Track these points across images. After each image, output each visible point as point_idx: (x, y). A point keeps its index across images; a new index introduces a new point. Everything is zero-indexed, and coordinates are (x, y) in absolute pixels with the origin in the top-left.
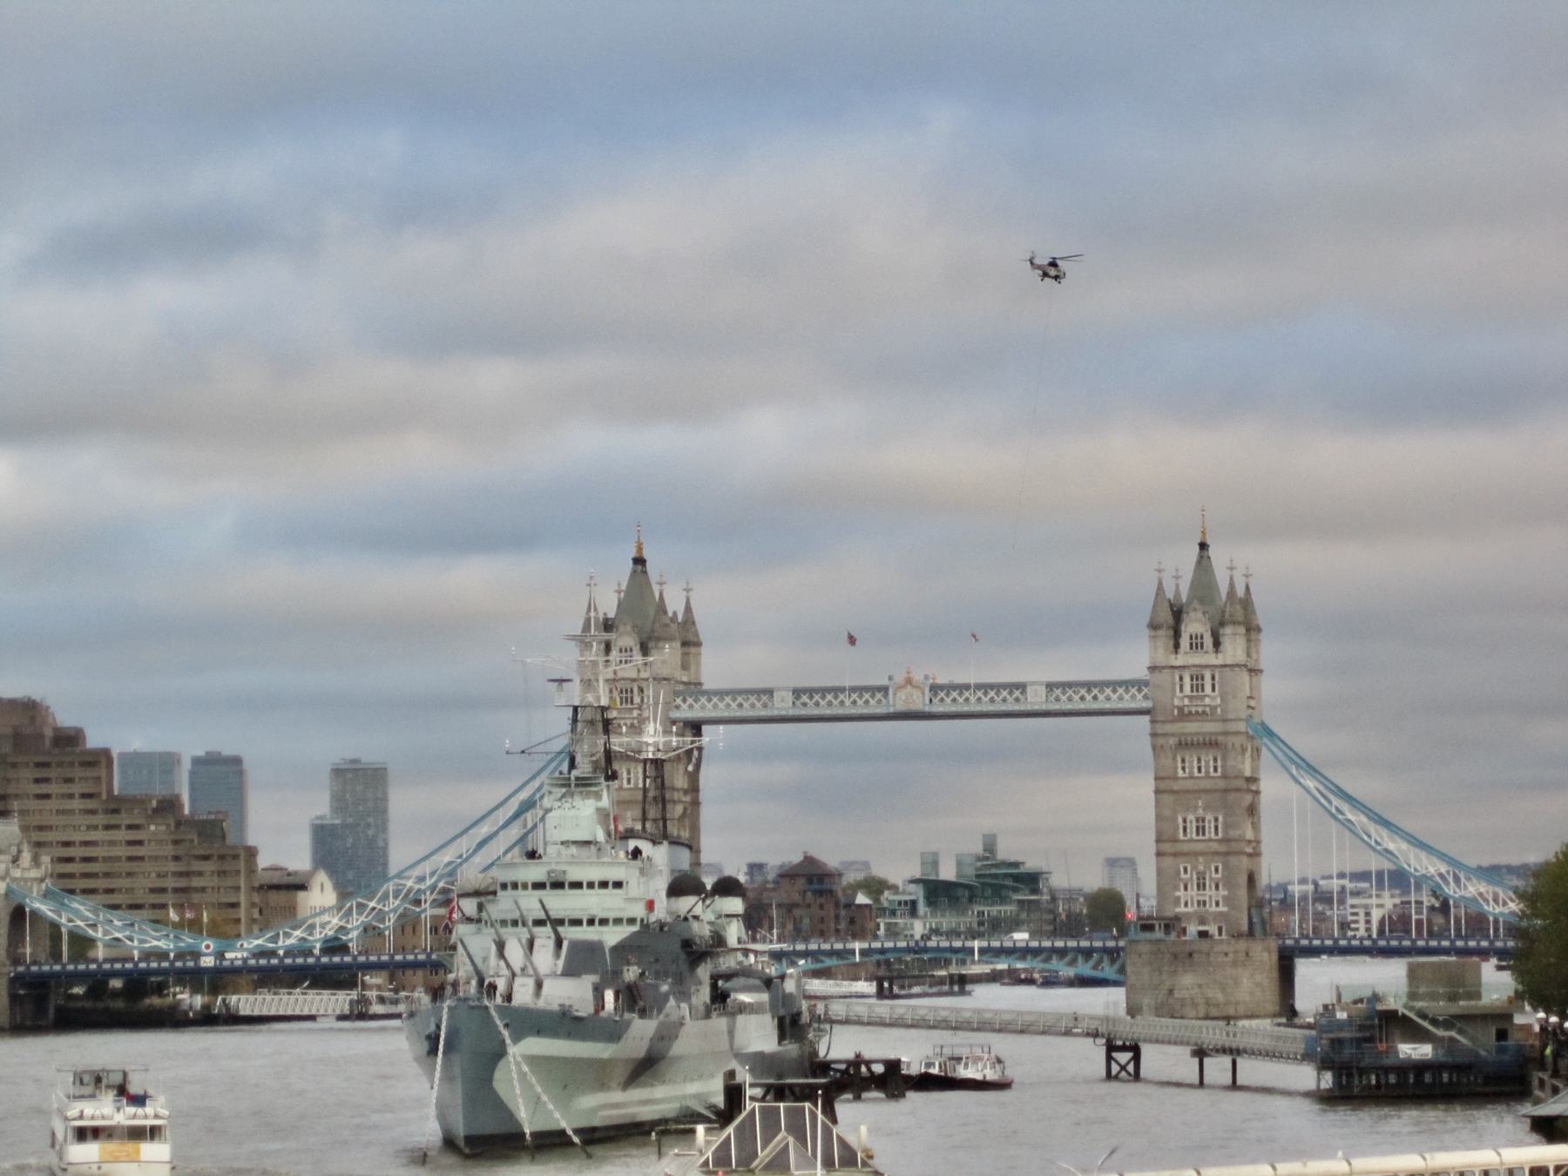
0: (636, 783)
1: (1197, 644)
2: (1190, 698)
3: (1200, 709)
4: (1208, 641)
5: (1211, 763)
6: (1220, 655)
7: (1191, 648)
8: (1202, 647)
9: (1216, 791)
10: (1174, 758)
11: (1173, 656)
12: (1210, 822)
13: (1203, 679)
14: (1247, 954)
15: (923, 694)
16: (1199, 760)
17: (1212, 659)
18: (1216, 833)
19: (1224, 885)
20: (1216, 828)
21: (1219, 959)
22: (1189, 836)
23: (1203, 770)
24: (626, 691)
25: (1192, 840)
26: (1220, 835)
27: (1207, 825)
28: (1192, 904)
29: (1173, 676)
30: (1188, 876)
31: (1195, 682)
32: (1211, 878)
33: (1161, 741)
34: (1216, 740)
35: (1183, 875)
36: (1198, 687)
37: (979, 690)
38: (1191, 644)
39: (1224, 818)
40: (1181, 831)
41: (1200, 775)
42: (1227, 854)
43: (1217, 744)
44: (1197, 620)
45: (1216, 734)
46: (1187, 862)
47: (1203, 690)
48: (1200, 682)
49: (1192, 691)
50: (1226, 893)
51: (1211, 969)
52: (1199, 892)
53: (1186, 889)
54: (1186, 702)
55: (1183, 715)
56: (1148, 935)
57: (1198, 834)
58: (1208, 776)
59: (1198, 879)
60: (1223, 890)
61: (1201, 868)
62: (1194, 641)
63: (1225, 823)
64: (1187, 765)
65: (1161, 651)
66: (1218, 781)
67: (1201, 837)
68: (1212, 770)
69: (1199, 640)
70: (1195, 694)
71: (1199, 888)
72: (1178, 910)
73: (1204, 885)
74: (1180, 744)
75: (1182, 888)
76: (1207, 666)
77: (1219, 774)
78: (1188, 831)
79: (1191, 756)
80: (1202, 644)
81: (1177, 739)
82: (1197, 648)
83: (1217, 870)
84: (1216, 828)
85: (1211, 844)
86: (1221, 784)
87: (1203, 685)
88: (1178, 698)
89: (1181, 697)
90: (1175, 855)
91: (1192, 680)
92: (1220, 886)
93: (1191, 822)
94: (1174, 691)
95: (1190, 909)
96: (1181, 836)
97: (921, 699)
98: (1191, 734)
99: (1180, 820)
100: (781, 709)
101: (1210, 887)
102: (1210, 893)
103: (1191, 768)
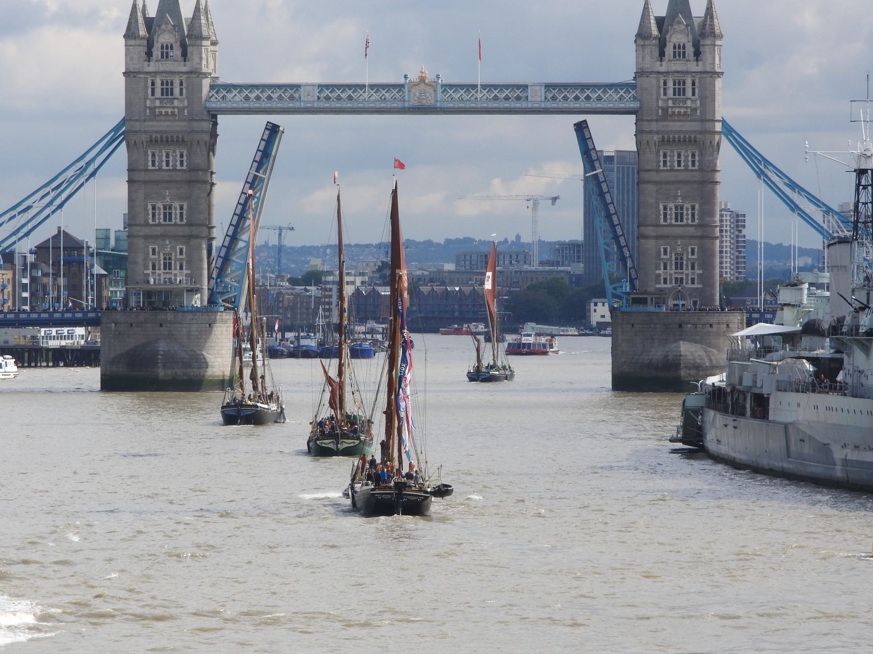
0: (174, 165)
1: (680, 53)
2: (674, 100)
3: (682, 111)
4: (690, 50)
5: (690, 158)
6: (700, 63)
7: (675, 56)
8: (684, 57)
9: (695, 182)
10: (658, 152)
11: (658, 63)
12: (687, 209)
13: (684, 84)
14: (728, 326)
15: (435, 91)
16: (679, 155)
17: (693, 67)
18: (693, 220)
19: (699, 265)
20: (693, 215)
21: (705, 330)
22: (669, 221)
23: (682, 164)
24: (167, 83)
25: (671, 225)
26: (697, 221)
27: (685, 212)
28: (671, 280)
29: (658, 81)
30: (695, 257)
31: (677, 87)
32: (688, 259)
33: (647, 137)
34: (695, 137)
35: (662, 256)
36: (680, 91)
37: (484, 90)
38: (675, 53)
39: (699, 206)
40: (662, 217)
41: (679, 168)
42: (702, 237)
43: (695, 141)
44: (681, 32)
45: (695, 132)
46: (667, 244)
47: (684, 95)
48: (681, 86)
49: (674, 94)
50: (701, 272)
51: (698, 338)
52: (676, 271)
53: (665, 268)
54: (670, 103)
55: (666, 115)
56: (641, 308)
57: (676, 220)
59: (676, 259)
60: (699, 269)
61: (679, 249)
62: (677, 50)
63: (701, 210)
64: (668, 159)
65: (648, 59)
66: (695, 173)
67: (679, 223)
68: (690, 164)
69: (682, 50)
70: (677, 97)
71: (676, 268)
72: (658, 286)
73: (682, 264)
74: (663, 141)
75: (662, 267)
76: (687, 72)
77: (696, 168)
78: (668, 217)
79: (687, 151)
80: (684, 53)
81: (660, 136)
82: (679, 56)
83: (693, 253)
84: (693, 215)
85: (688, 229)
87: (684, 89)
88: (662, 99)
89: (667, 99)
90: (657, 237)
91: (674, 84)
92: (696, 267)
93: (671, 209)
94: (658, 94)
95: (668, 286)
96: (662, 222)
97: (433, 95)
98: (672, 132)
99: (661, 207)
100: (308, 102)
101: (687, 266)
102: (687, 272)
103: (672, 161)
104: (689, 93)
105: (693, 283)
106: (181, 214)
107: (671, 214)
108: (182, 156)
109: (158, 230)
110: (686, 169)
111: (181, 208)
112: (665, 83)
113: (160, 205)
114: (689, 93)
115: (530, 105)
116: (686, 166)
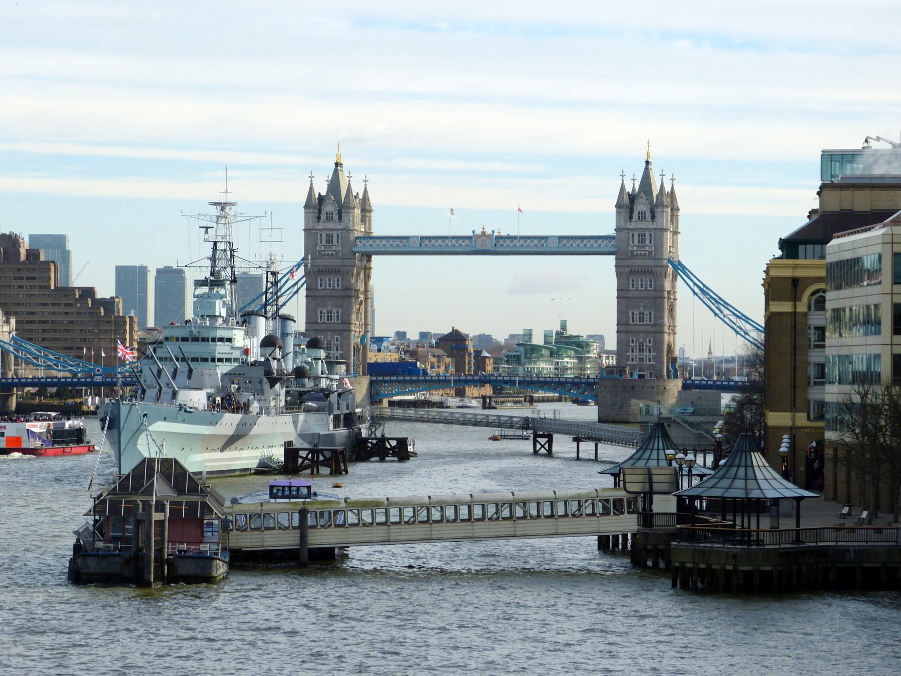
2: (638, 247)
4: (648, 215)
5: (648, 283)
11: (629, 223)
13: (645, 236)
18: (650, 322)
20: (650, 318)
25: (636, 325)
35: (631, 344)
44: (643, 203)
53: (633, 352)
54: (635, 248)
58: (646, 290)
61: (641, 340)
83: (650, 342)
84: (650, 318)
86: (653, 294)
95: (634, 363)
103: (637, 285)
104: (647, 242)
105: (650, 361)
106: (338, 316)
107: (637, 317)
108: (338, 281)
109: (324, 327)
110: (646, 290)
111: (338, 313)
112: (633, 236)
113: (325, 311)
114: (647, 242)
115: (549, 249)
116: (646, 287)
